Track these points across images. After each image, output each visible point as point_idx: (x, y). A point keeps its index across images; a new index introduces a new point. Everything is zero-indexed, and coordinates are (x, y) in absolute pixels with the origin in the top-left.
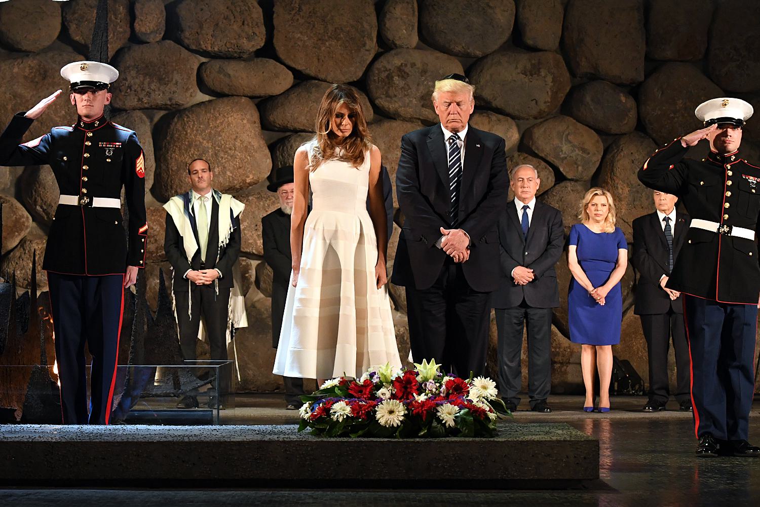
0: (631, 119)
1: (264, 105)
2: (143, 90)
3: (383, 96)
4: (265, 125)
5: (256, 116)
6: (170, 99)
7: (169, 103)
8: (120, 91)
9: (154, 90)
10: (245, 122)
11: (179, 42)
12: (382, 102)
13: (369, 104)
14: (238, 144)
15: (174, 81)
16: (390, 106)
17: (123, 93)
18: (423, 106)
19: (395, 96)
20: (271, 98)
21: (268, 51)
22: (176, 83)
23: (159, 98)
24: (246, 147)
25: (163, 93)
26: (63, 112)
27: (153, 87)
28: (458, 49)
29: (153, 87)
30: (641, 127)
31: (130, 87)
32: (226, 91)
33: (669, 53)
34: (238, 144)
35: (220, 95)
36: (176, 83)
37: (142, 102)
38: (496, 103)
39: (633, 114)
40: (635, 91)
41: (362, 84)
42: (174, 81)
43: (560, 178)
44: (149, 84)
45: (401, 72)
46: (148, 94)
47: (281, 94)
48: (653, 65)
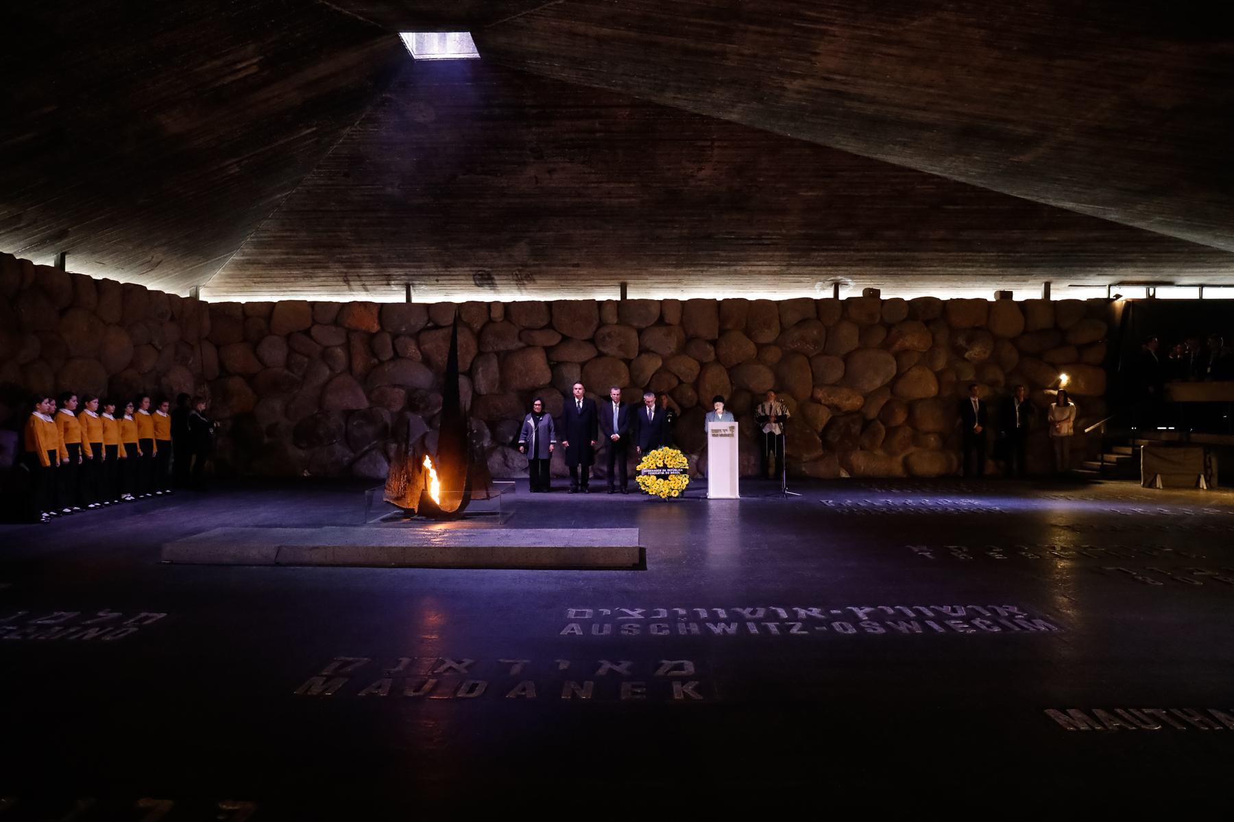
0: (712, 356)
1: (548, 350)
4: (549, 360)
11: (510, 322)
12: (601, 348)
16: (605, 350)
20: (552, 347)
21: (550, 326)
28: (635, 324)
30: (718, 360)
33: (729, 326)
35: (529, 346)
39: (713, 354)
40: (714, 343)
41: (592, 341)
43: (681, 382)
45: (609, 335)
48: (722, 332)
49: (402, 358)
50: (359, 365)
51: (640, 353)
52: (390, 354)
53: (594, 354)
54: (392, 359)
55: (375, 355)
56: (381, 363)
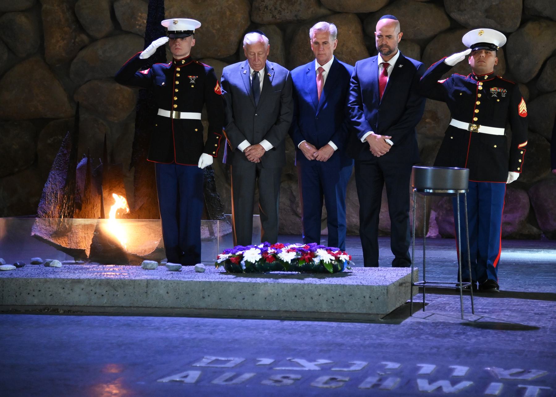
2: (276, 9)
3: (456, 10)
5: (359, 28)
6: (296, 16)
7: (295, 19)
8: (260, 10)
9: (284, 9)
10: (351, 32)
12: (455, 15)
13: (445, 17)
14: (344, 49)
15: (299, 2)
17: (261, 12)
18: (487, 17)
19: (465, 10)
22: (300, 4)
23: (288, 15)
24: (351, 51)
25: (291, 12)
26: (218, 26)
27: (283, 6)
29: (283, 6)
31: (266, 7)
32: (338, 9)
34: (344, 49)
36: (300, 4)
37: (276, 18)
38: (546, 13)
42: (299, 2)
44: (281, 4)
46: (280, 12)
47: (377, 11)
49: (128, 33)
50: (58, 44)
51: (523, 23)
52: (108, 27)
53: (447, 24)
54: (109, 36)
55: (81, 28)
56: (93, 40)
